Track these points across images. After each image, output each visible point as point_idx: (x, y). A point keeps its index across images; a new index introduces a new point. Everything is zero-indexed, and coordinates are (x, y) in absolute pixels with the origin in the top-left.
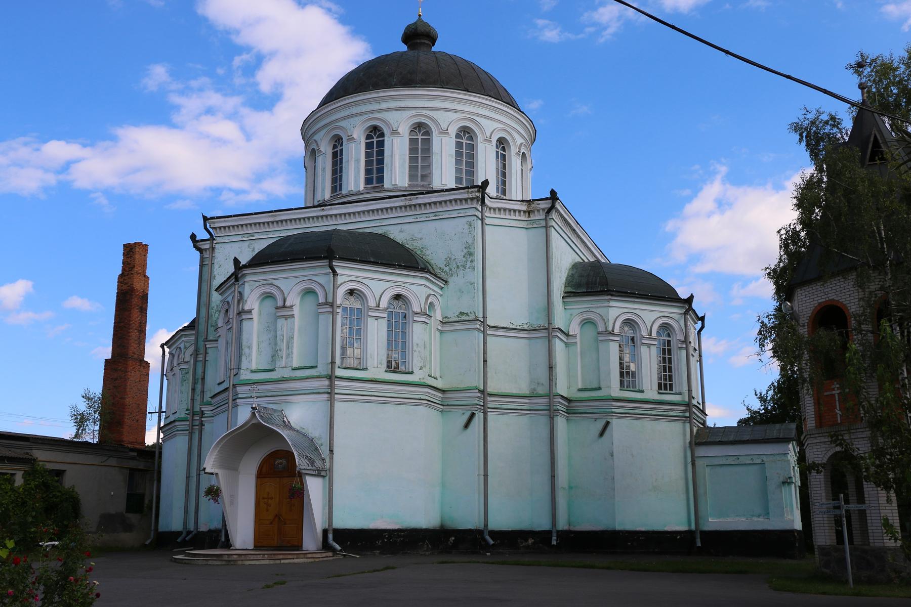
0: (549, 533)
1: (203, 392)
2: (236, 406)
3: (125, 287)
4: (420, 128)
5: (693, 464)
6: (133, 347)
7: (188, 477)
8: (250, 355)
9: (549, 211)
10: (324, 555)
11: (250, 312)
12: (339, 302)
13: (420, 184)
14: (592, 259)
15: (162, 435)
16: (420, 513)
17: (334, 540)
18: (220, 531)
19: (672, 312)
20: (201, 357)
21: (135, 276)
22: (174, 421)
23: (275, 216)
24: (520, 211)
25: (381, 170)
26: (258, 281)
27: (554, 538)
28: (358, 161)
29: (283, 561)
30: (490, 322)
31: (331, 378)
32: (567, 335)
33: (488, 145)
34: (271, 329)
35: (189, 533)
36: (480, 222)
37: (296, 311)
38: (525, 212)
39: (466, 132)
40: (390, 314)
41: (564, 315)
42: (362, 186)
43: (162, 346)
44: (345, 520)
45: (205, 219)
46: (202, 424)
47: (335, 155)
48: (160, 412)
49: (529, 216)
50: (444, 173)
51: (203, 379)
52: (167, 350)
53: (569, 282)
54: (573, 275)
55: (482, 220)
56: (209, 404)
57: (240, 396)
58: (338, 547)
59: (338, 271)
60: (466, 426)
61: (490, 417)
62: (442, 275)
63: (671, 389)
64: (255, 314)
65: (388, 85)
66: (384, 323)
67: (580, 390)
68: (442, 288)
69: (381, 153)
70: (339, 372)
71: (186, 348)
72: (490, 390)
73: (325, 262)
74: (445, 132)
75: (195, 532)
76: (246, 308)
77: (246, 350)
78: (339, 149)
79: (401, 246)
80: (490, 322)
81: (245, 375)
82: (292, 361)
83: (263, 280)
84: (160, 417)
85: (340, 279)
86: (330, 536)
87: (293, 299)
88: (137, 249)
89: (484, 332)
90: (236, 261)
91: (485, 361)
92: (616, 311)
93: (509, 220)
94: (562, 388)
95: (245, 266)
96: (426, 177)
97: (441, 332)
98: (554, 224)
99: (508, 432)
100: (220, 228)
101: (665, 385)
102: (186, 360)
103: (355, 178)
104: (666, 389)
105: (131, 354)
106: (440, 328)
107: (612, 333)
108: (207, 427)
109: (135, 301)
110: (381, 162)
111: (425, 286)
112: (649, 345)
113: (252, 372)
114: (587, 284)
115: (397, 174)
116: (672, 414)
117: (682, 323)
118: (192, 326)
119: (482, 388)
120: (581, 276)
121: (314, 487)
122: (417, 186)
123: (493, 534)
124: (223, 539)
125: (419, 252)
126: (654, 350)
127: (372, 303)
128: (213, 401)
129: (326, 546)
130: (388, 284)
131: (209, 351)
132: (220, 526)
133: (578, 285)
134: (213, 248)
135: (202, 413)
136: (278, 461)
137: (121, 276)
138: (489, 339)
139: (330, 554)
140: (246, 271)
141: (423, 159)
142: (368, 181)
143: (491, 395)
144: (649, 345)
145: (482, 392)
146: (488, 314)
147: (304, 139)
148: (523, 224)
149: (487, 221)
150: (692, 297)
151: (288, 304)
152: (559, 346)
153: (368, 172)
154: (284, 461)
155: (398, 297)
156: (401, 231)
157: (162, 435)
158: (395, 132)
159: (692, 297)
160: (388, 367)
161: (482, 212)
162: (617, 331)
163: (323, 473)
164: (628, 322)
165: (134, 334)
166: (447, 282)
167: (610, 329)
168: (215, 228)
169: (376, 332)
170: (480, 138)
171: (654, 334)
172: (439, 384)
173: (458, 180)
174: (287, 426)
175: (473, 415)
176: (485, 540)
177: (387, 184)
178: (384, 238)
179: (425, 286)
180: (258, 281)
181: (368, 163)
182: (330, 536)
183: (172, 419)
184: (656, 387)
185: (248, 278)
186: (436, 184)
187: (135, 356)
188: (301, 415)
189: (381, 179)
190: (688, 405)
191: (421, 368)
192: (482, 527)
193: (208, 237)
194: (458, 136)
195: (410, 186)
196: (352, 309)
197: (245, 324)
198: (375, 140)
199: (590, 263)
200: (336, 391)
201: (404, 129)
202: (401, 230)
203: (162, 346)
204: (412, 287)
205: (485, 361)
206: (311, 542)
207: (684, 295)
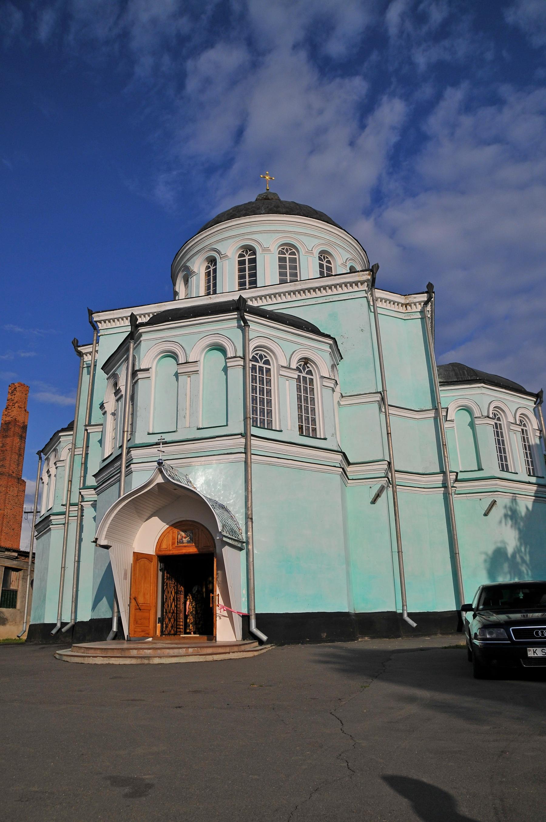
2: (129, 473)
7: (63, 568)
17: (258, 627)
23: (160, 306)
35: (64, 624)
37: (201, 367)
39: (324, 255)
47: (208, 274)
57: (134, 461)
58: (264, 638)
60: (374, 502)
73: (235, 315)
74: (310, 252)
75: (73, 623)
78: (212, 268)
83: (161, 338)
86: (253, 622)
95: (142, 325)
99: (421, 506)
100: (105, 321)
113: (149, 434)
124: (115, 628)
129: (247, 634)
130: (297, 347)
140: (142, 330)
150: (542, 392)
155: (306, 361)
159: (542, 392)
166: (342, 358)
182: (253, 622)
196: (261, 368)
198: (247, 258)
201: (275, 249)
206: (226, 631)
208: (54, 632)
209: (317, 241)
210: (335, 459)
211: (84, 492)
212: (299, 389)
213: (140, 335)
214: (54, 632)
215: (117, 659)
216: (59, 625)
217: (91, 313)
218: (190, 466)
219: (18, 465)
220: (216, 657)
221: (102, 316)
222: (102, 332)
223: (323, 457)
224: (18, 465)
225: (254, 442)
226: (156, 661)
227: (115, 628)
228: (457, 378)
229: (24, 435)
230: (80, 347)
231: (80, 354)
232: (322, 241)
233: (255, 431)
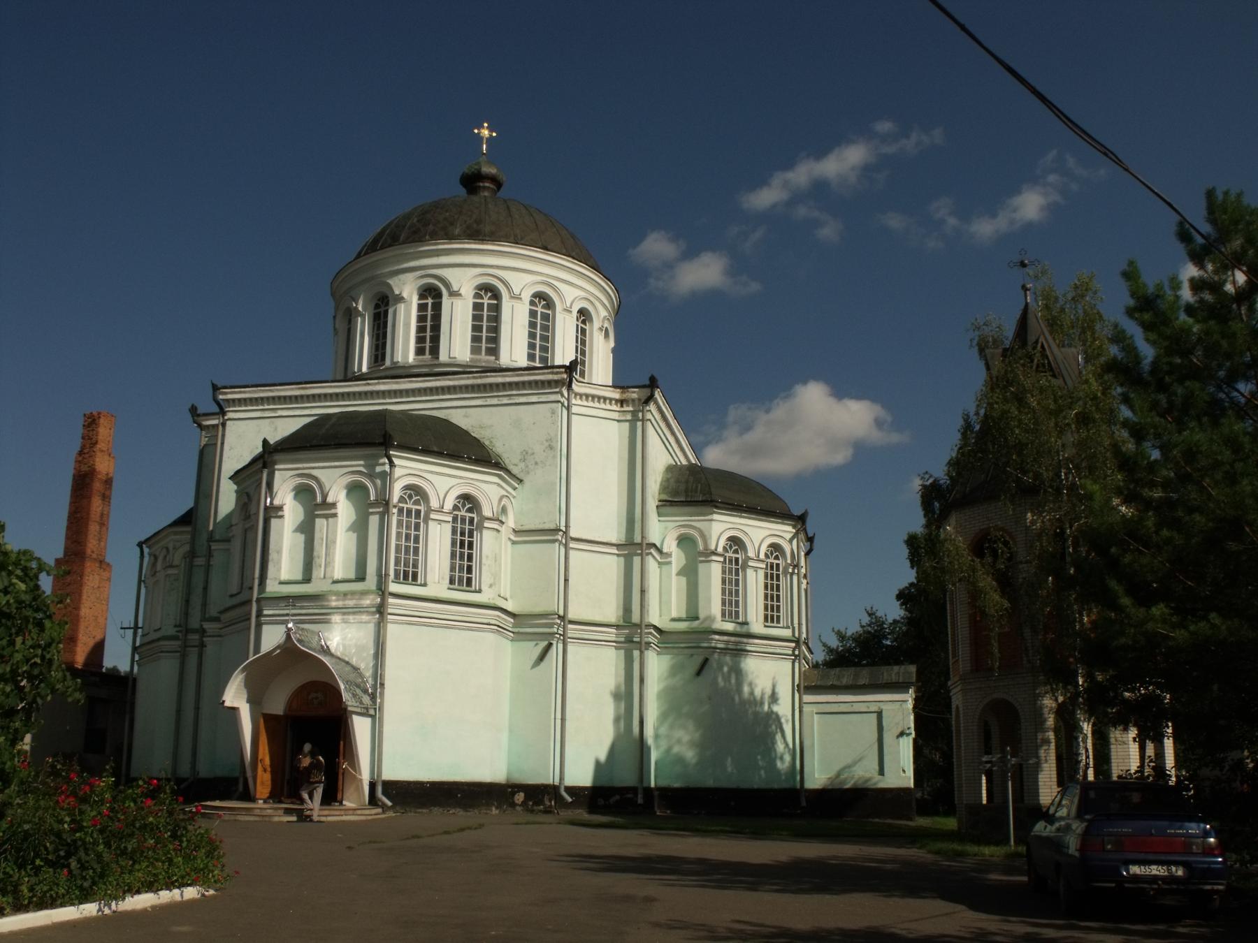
0: (633, 790)
1: (204, 605)
2: (259, 626)
3: (85, 468)
4: (490, 292)
5: (801, 711)
6: (92, 544)
7: (179, 712)
8: (279, 562)
9: (647, 402)
10: (367, 812)
11: (280, 508)
12: (395, 499)
13: (485, 359)
14: (684, 462)
15: (137, 657)
16: (485, 764)
17: (384, 793)
18: (236, 780)
19: (783, 532)
20: (200, 561)
21: (98, 454)
22: (159, 640)
24: (611, 400)
25: (436, 339)
27: (640, 796)
28: (407, 325)
29: (330, 819)
30: (573, 534)
32: (660, 551)
33: (566, 315)
34: (307, 529)
36: (565, 412)
38: (617, 401)
39: (542, 298)
40: (455, 519)
41: (662, 530)
42: (411, 358)
43: (140, 545)
44: (394, 771)
45: (215, 388)
46: (202, 645)
48: (136, 628)
50: (514, 349)
51: (205, 589)
52: (146, 550)
53: (664, 488)
54: (668, 480)
55: (568, 409)
56: (217, 619)
58: (389, 804)
59: (396, 461)
61: (570, 648)
62: (515, 470)
63: (778, 622)
64: (287, 511)
65: (451, 238)
66: (448, 528)
67: (674, 620)
68: (515, 489)
69: (437, 317)
70: (394, 587)
71: (174, 548)
72: (572, 615)
73: (381, 451)
74: (517, 298)
77: (273, 555)
79: (466, 433)
80: (573, 533)
81: (272, 587)
82: (333, 571)
84: (135, 634)
85: (398, 472)
87: (338, 495)
88: (102, 421)
89: (566, 546)
90: (265, 442)
91: (566, 580)
92: (720, 526)
93: (599, 409)
94: (654, 617)
96: (494, 351)
97: (514, 543)
98: (649, 416)
99: (594, 670)
101: (772, 617)
102: (176, 562)
103: (405, 349)
104: (772, 621)
105: (89, 551)
106: (513, 538)
107: (714, 553)
108: (210, 649)
109: (97, 485)
110: (436, 328)
111: (499, 485)
112: (756, 569)
113: (281, 583)
114: (686, 491)
115: (457, 344)
116: (778, 651)
117: (795, 542)
118: (187, 519)
119: (561, 613)
120: (678, 481)
121: (361, 727)
122: (480, 361)
123: (570, 790)
125: (487, 443)
126: (761, 574)
127: (434, 504)
128: (223, 617)
129: (373, 800)
131: (215, 554)
132: (237, 774)
133: (675, 493)
134: (224, 425)
135: (203, 632)
136: (313, 695)
137: (81, 453)
138: (572, 553)
139: (380, 810)
141: (489, 329)
142: (420, 351)
143: (571, 622)
144: (756, 569)
145: (562, 618)
146: (572, 524)
147: (333, 294)
148: (616, 416)
149: (574, 409)
151: (330, 499)
152: (652, 565)
153: (420, 340)
155: (466, 498)
156: (466, 416)
157: (137, 657)
158: (454, 294)
160: (452, 581)
161: (568, 400)
162: (720, 550)
163: (372, 712)
164: (736, 543)
165: (93, 528)
166: (521, 481)
167: (713, 548)
169: (438, 539)
170: (559, 307)
171: (762, 556)
172: (509, 606)
173: (531, 357)
174: (326, 651)
175: (550, 645)
176: (562, 798)
177: (443, 357)
178: (446, 423)
179: (499, 485)
181: (421, 329)
183: (147, 639)
184: (761, 618)
186: (505, 360)
187: (94, 556)
188: (343, 638)
189: (435, 351)
190: (797, 642)
191: (491, 586)
192: (557, 783)
193: (217, 410)
194: (532, 303)
195: (472, 360)
196: (409, 512)
197: (274, 522)
199: (682, 466)
200: (390, 611)
202: (467, 415)
203: (140, 545)
204: (483, 486)
205: (566, 580)
207: (797, 512)
209: (529, 278)
211: (206, 625)
212: (454, 531)
217: (215, 388)
219: (100, 540)
220: (330, 819)
224: (100, 540)
228: (687, 496)
229: (107, 493)
232: (539, 278)
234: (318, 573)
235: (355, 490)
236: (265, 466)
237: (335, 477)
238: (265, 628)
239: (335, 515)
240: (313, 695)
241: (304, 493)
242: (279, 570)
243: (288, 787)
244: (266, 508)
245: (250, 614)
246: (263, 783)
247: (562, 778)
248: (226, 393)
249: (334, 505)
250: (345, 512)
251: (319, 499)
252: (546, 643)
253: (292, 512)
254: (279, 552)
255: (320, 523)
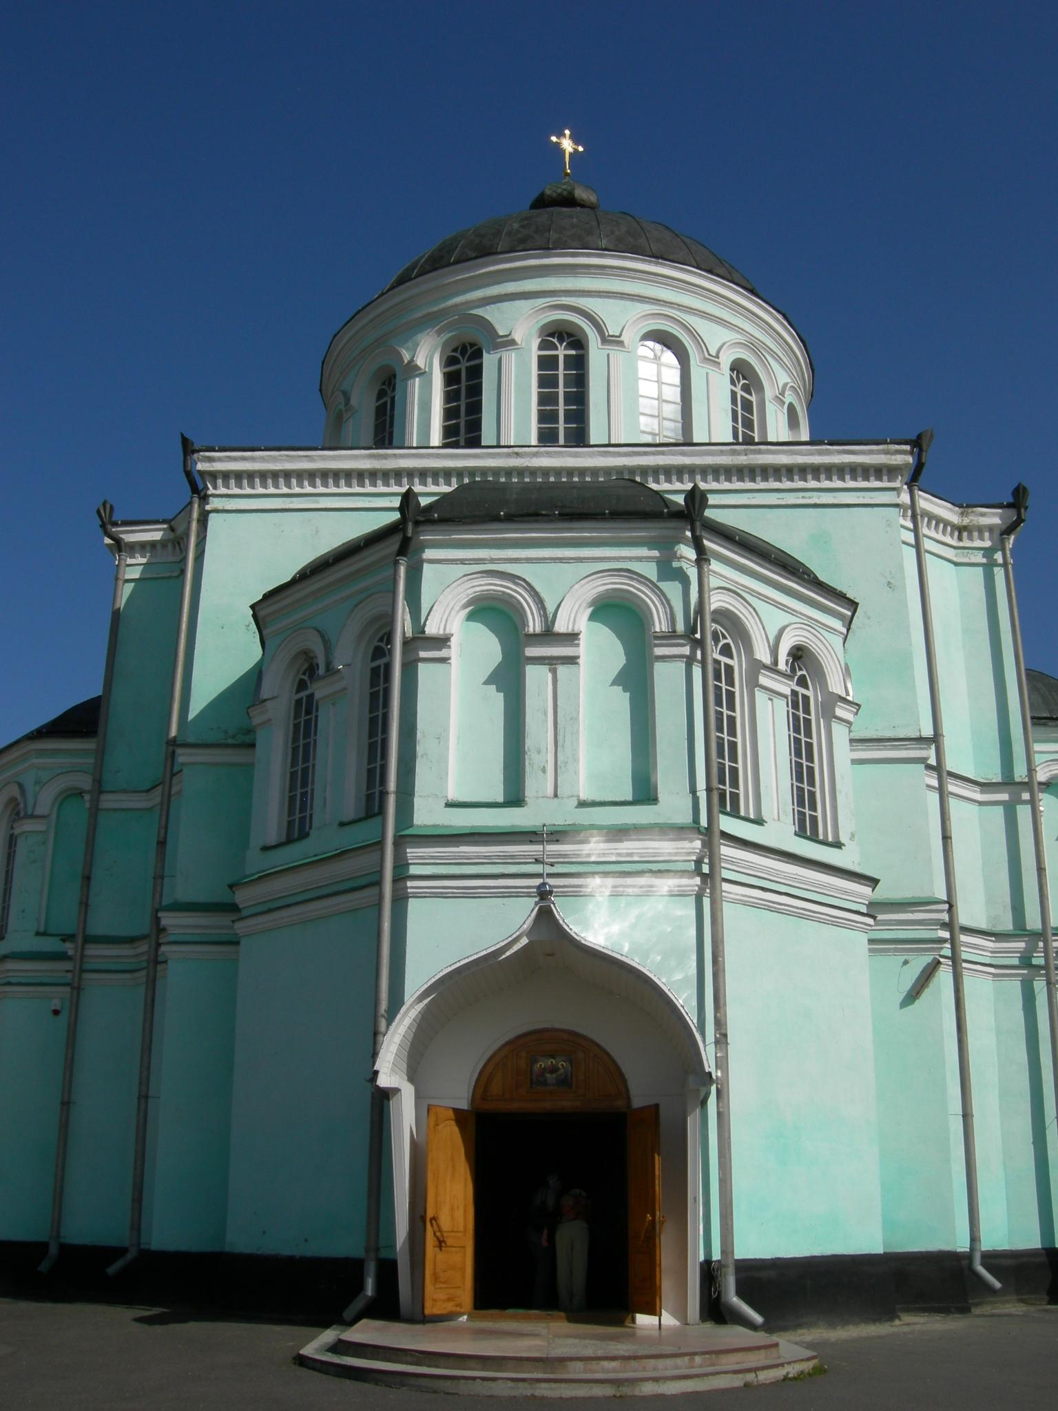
2: (401, 900)
17: (740, 1293)
26: (462, 562)
31: (710, 836)
37: (583, 651)
49: (960, 539)
57: (414, 870)
74: (713, 360)
76: (432, 629)
100: (226, 476)
113: (450, 805)
130: (786, 618)
154: (561, 1063)
168: (214, 475)
180: (462, 562)
185: (429, 554)
192: (961, 1244)
208: (44, 1267)
210: (861, 896)
213: (423, 546)
214: (44, 1267)
215: (553, 1385)
216: (53, 1250)
217: (188, 448)
218: (577, 895)
221: (220, 460)
222: (214, 503)
223: (837, 889)
225: (727, 851)
226: (648, 1389)
227: (370, 1288)
230: (115, 524)
231: (119, 546)
233: (727, 824)
234: (537, 784)
235: (617, 611)
236: (403, 550)
237: (568, 579)
238: (413, 904)
239: (572, 660)
240: (542, 1063)
241: (494, 612)
242: (443, 776)
243: (509, 1278)
244: (406, 643)
245: (380, 872)
246: (451, 1269)
247: (974, 1239)
248: (211, 460)
249: (572, 638)
250: (599, 651)
251: (534, 625)
252: (927, 959)
253: (471, 651)
254: (442, 738)
255: (536, 677)
